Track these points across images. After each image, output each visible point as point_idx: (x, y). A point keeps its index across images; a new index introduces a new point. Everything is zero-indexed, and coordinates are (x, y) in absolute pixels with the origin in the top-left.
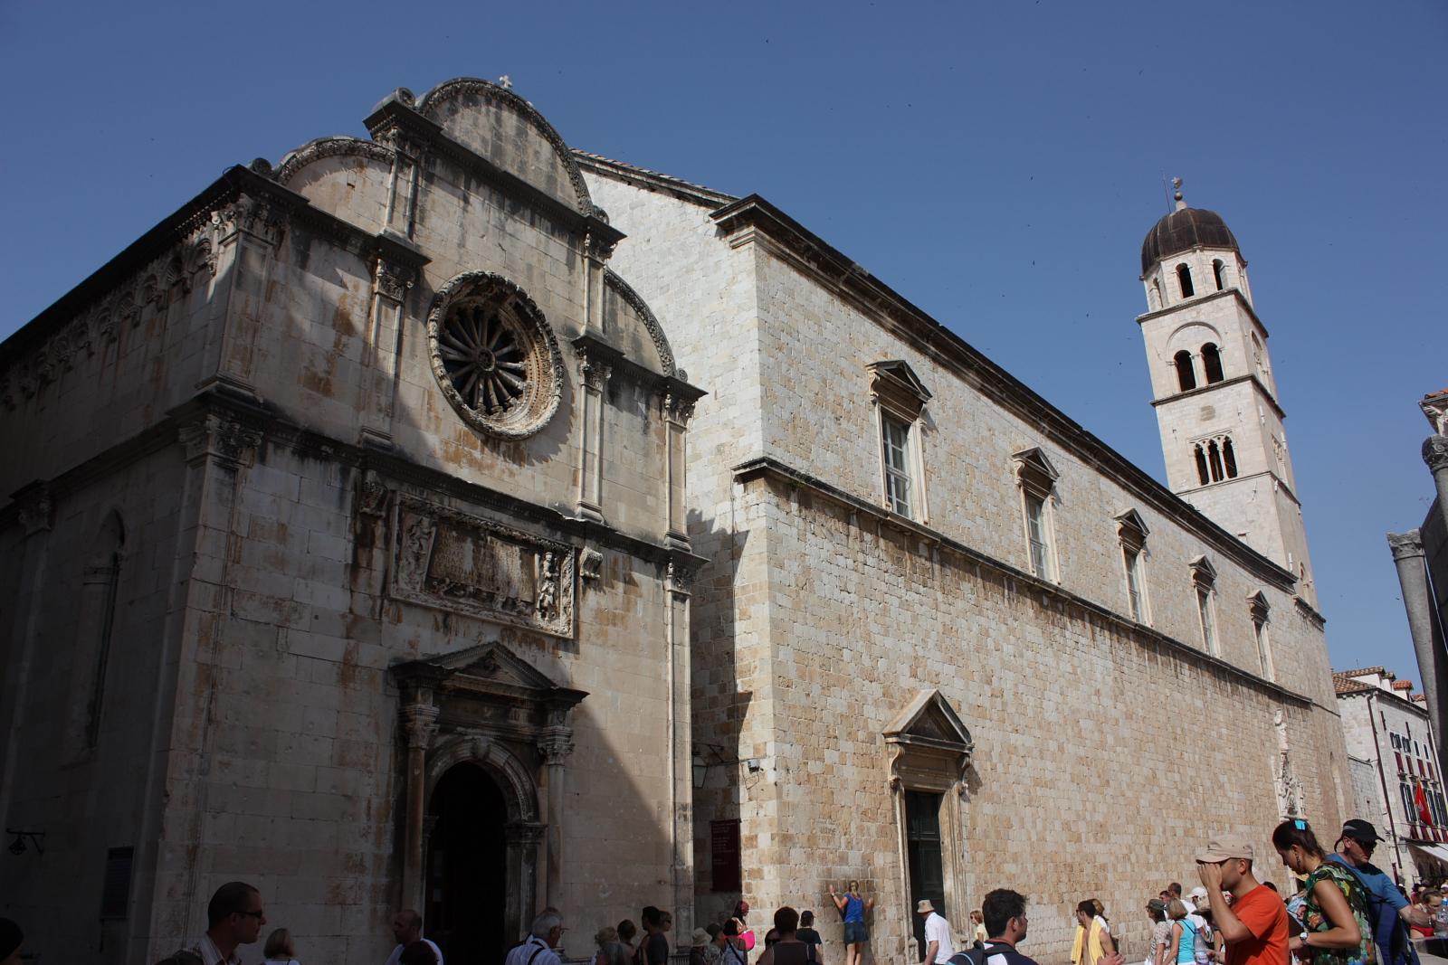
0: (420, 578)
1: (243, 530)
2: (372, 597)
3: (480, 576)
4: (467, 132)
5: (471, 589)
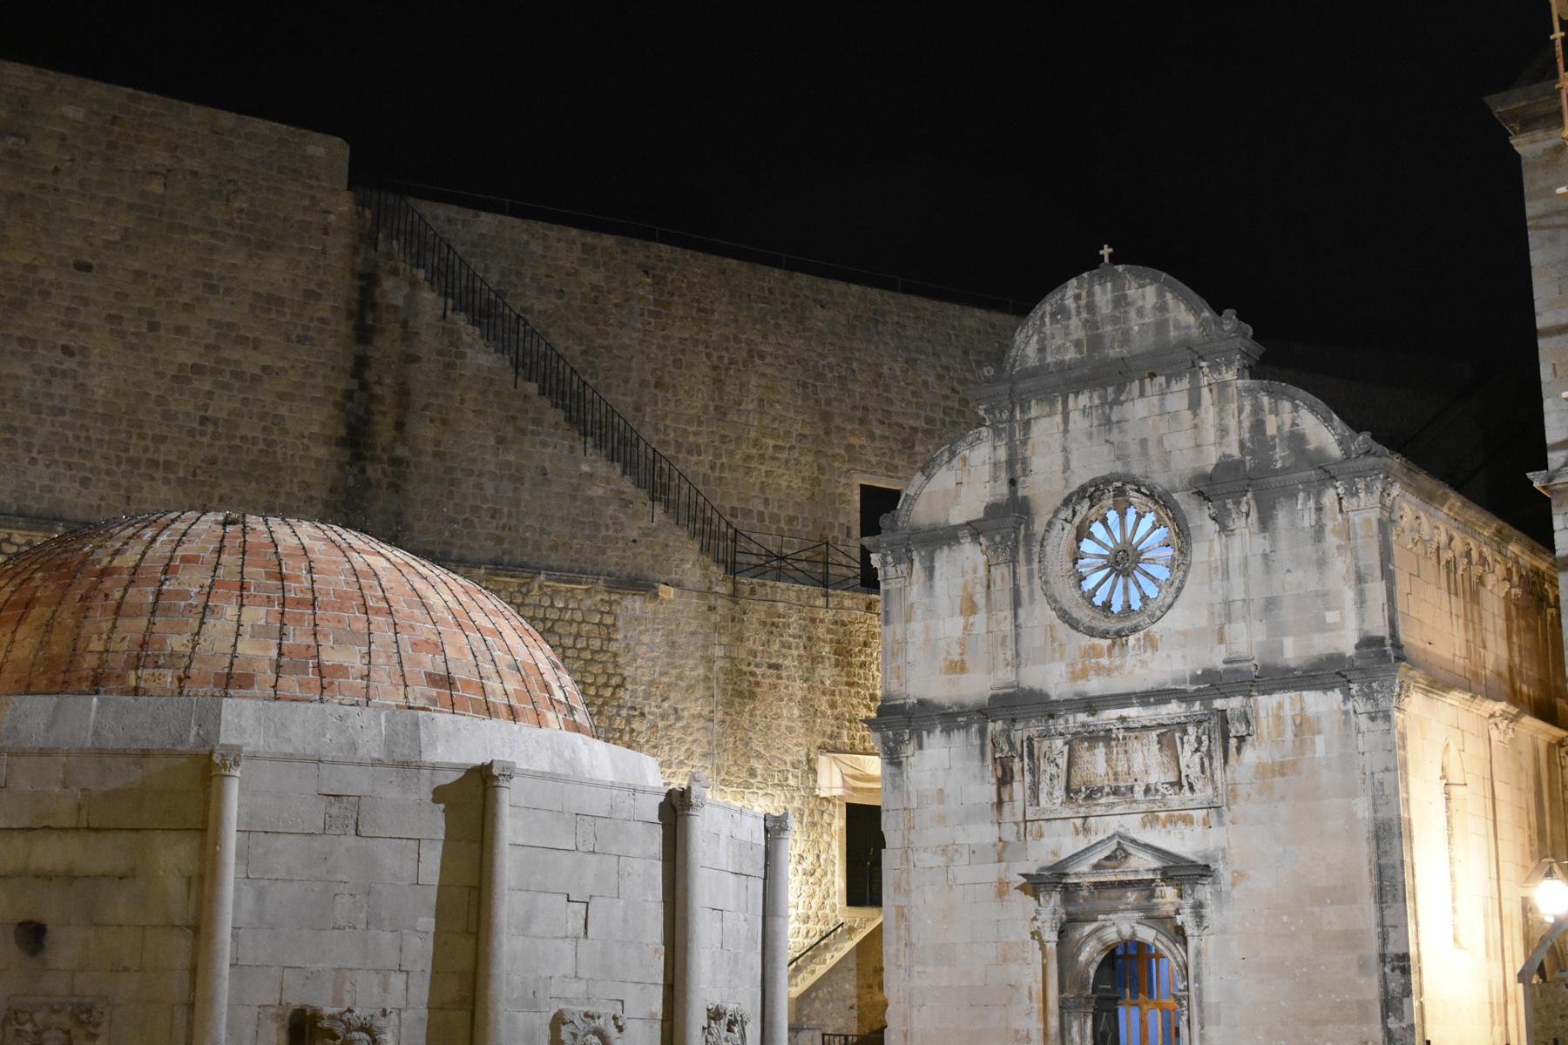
0: (1059, 793)
1: (914, 804)
2: (1016, 823)
3: (1116, 774)
4: (1059, 348)
5: (1107, 789)
